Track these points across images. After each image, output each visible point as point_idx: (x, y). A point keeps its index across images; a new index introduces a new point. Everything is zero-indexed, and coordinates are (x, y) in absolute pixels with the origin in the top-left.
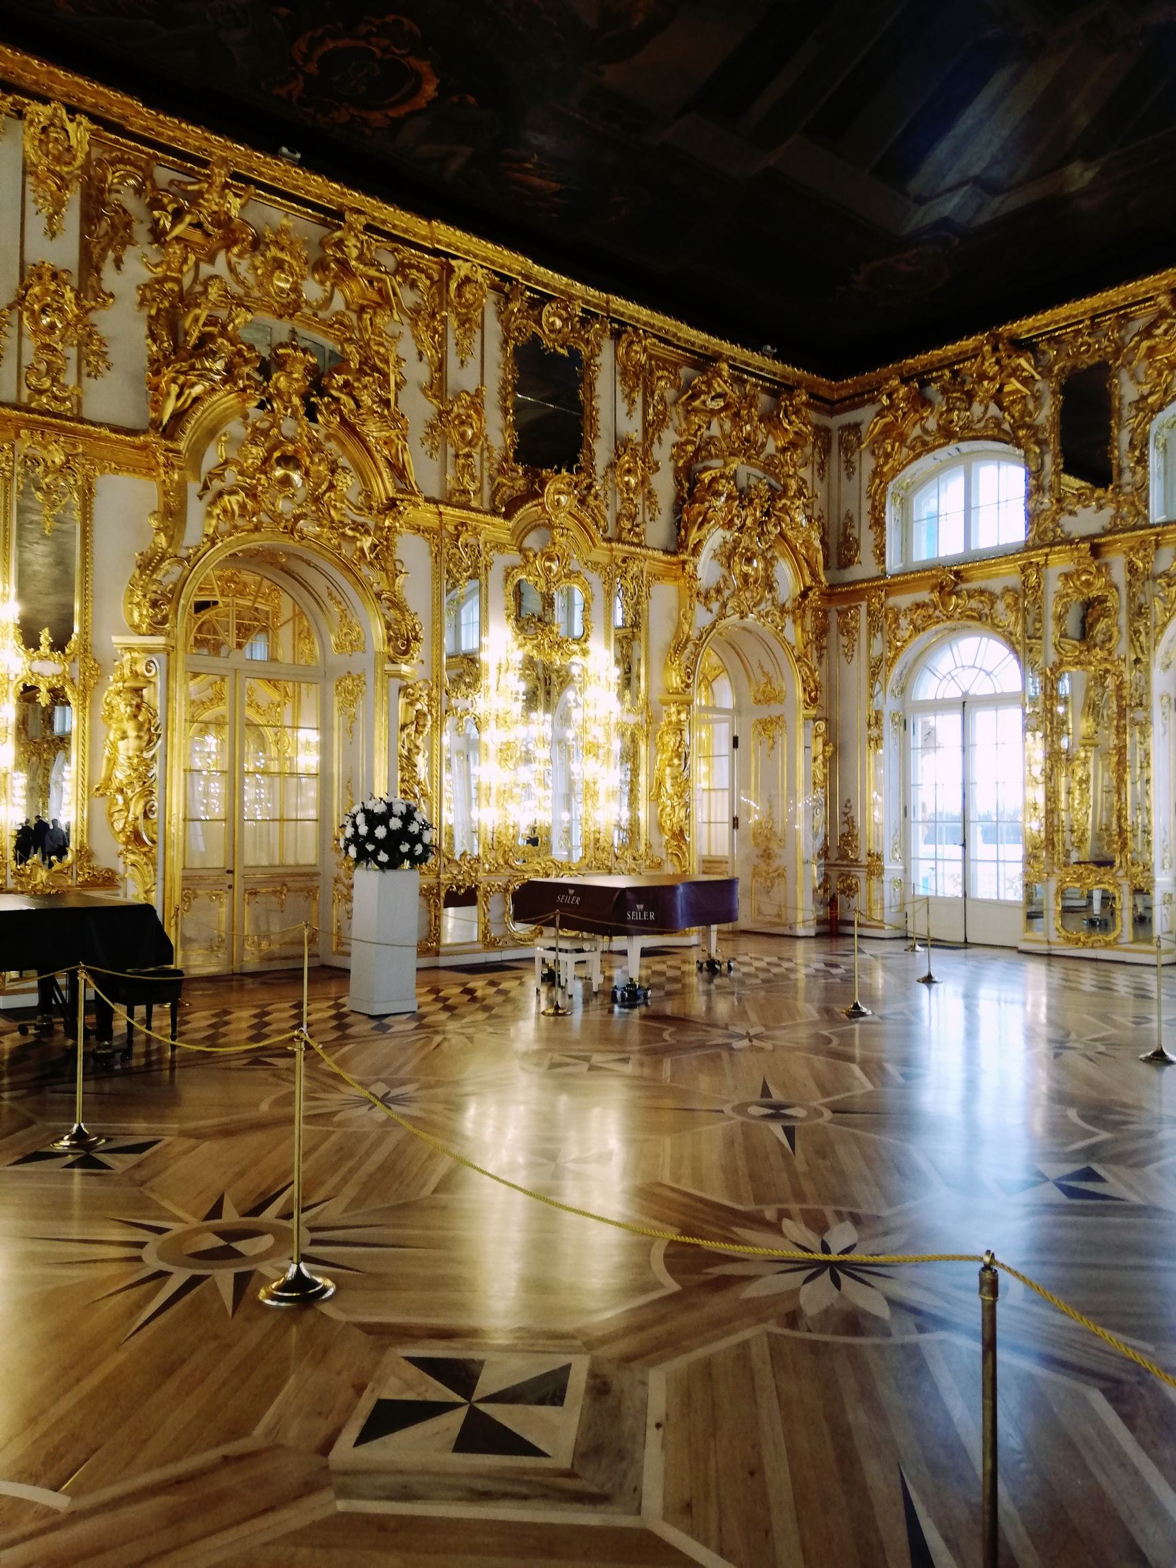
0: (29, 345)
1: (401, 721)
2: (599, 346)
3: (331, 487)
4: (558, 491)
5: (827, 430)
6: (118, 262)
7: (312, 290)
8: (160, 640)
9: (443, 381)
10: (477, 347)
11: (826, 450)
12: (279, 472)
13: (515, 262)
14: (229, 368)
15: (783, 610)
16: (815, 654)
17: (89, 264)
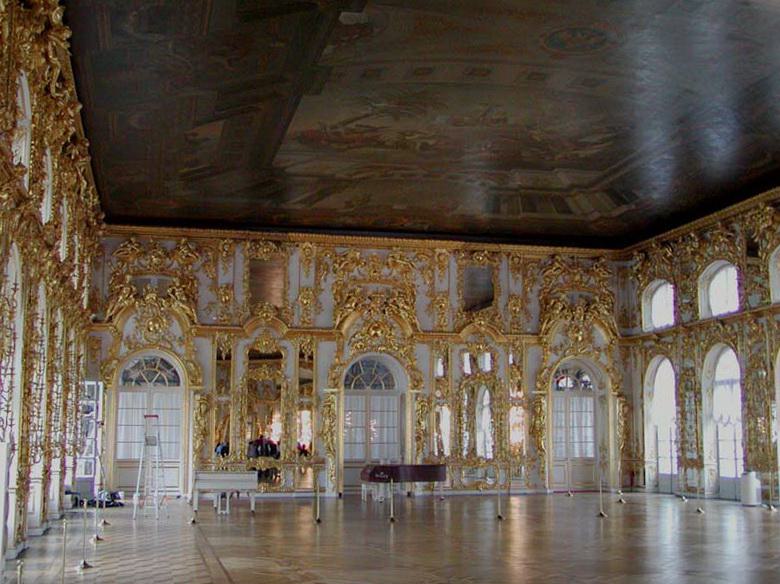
0: (301, 309)
1: (416, 408)
2: (501, 261)
3: (390, 335)
4: (481, 322)
5: (625, 267)
6: (325, 280)
7: (385, 271)
8: (335, 390)
9: (433, 289)
10: (447, 275)
11: (625, 276)
12: (373, 332)
13: (458, 244)
14: (356, 305)
15: (599, 349)
16: (622, 367)
17: (317, 282)
